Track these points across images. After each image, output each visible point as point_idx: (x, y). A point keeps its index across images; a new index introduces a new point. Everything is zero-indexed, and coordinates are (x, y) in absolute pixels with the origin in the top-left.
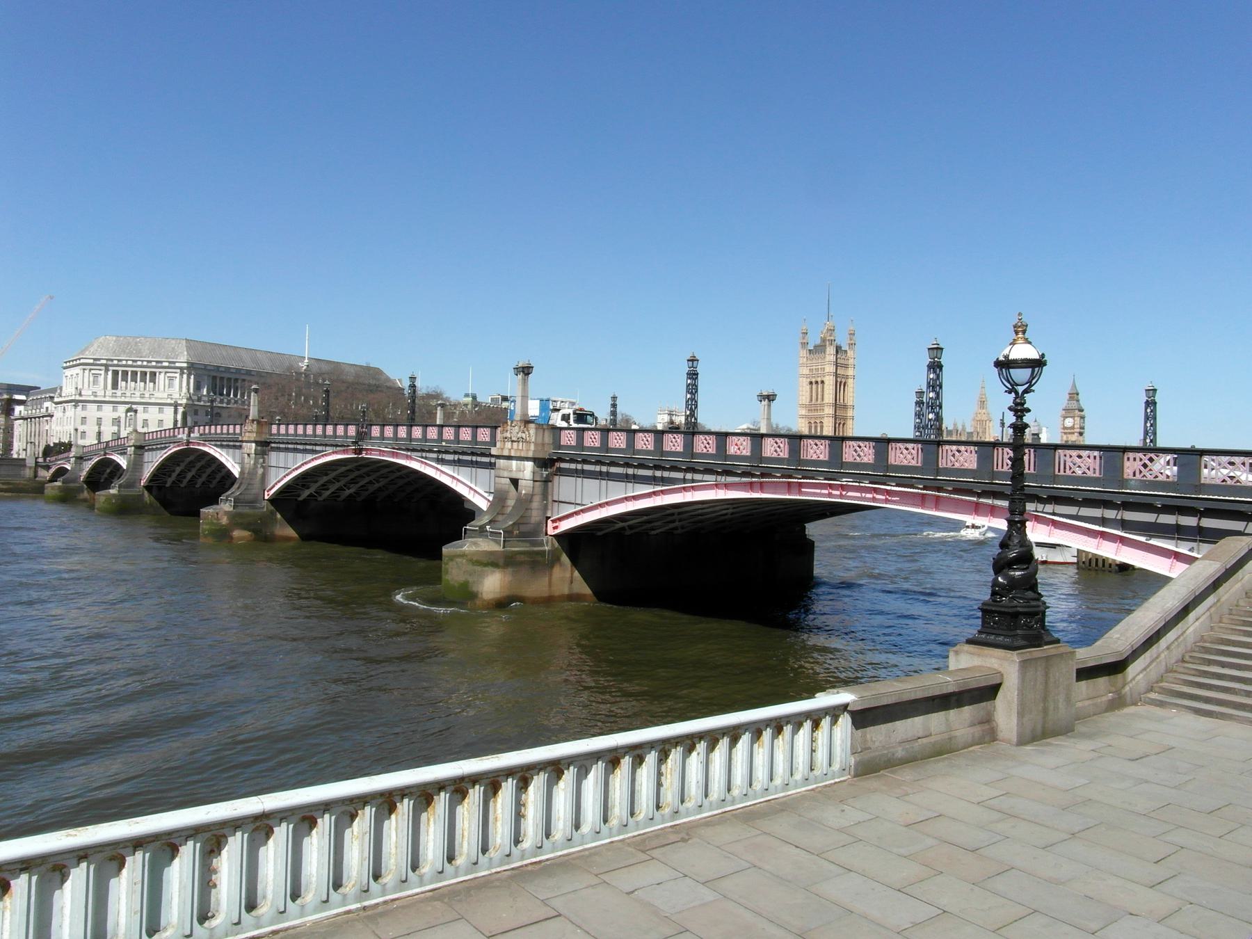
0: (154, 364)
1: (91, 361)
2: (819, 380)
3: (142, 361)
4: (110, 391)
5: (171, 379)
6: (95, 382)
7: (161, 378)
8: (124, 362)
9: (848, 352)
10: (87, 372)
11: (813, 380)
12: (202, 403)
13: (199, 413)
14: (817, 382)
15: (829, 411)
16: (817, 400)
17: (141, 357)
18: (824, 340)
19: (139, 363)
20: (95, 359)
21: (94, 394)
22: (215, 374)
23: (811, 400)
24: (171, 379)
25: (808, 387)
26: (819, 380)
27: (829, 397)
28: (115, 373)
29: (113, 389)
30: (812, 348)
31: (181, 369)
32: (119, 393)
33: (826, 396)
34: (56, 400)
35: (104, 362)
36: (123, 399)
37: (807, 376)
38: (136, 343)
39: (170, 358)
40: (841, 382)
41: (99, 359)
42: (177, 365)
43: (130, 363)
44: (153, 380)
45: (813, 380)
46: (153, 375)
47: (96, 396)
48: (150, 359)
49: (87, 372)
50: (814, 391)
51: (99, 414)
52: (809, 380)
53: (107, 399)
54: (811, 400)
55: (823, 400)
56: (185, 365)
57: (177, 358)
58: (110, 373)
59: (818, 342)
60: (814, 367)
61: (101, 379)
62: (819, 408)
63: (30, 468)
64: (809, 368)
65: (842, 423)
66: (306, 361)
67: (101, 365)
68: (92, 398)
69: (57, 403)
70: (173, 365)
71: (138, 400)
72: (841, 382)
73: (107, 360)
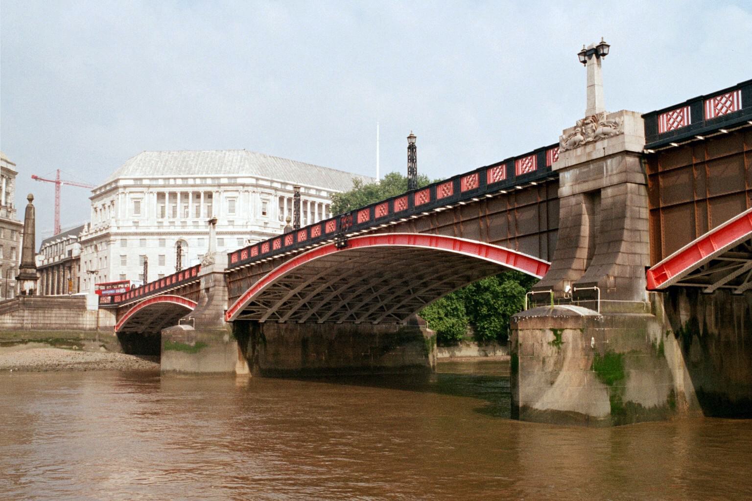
0: (209, 181)
1: (131, 182)
3: (194, 178)
19: (191, 182)
24: (232, 200)
28: (161, 196)
34: (83, 239)
36: (172, 229)
39: (229, 173)
42: (239, 181)
43: (179, 182)
46: (209, 195)
48: (204, 175)
53: (153, 230)
57: (238, 173)
63: (92, 312)
69: (82, 243)
73: (151, 179)
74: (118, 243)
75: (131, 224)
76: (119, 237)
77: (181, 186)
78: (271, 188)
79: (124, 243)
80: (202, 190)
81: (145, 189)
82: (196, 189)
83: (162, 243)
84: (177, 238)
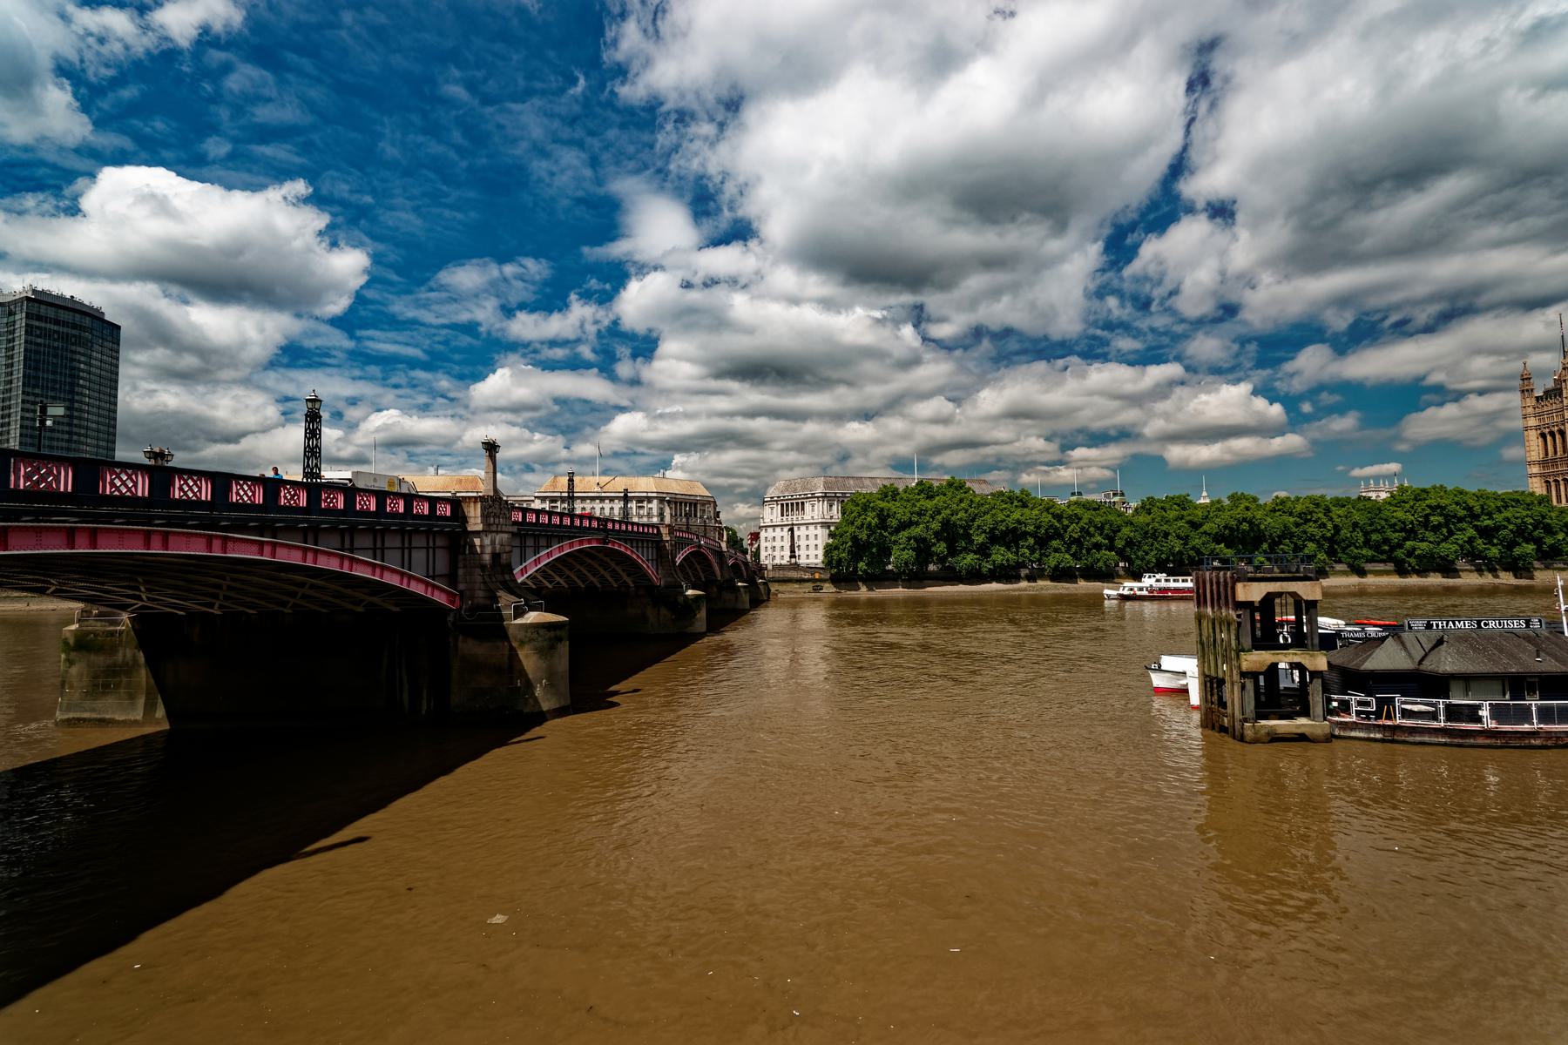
4: (779, 519)
5: (813, 505)
7: (807, 506)
16: (1556, 453)
23: (1547, 454)
24: (813, 505)
28: (782, 505)
30: (1541, 394)
31: (818, 497)
32: (785, 518)
37: (1537, 428)
44: (803, 509)
46: (803, 503)
52: (1539, 432)
54: (1547, 454)
59: (1550, 385)
83: (782, 530)
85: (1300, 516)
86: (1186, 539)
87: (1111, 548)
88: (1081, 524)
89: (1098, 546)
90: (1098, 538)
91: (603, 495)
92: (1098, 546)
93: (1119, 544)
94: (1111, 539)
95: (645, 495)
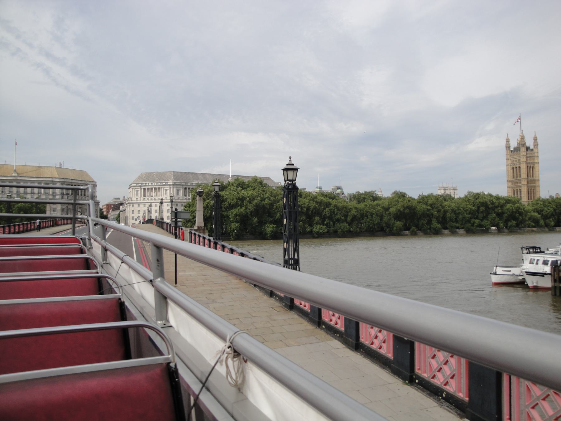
1: (135, 185)
2: (517, 166)
3: (155, 183)
4: (143, 198)
6: (137, 194)
8: (148, 184)
9: (534, 149)
10: (134, 189)
11: (514, 167)
12: (179, 201)
13: (178, 205)
14: (516, 167)
15: (524, 183)
16: (517, 177)
17: (154, 181)
18: (519, 144)
19: (154, 184)
20: (137, 184)
21: (137, 200)
22: (186, 187)
23: (514, 177)
25: (512, 171)
26: (517, 166)
27: (524, 175)
28: (144, 189)
29: (144, 197)
32: (146, 198)
33: (522, 175)
35: (140, 185)
36: (147, 201)
38: (153, 175)
40: (530, 167)
41: (138, 184)
43: (150, 184)
45: (514, 167)
46: (159, 189)
47: (137, 200)
48: (158, 182)
49: (134, 189)
50: (515, 173)
51: (139, 209)
52: (512, 167)
54: (514, 177)
55: (520, 177)
56: (171, 183)
58: (143, 189)
59: (516, 145)
60: (514, 160)
61: (139, 192)
62: (518, 182)
64: (511, 160)
65: (533, 189)
66: (230, 177)
67: (139, 186)
68: (136, 202)
70: (167, 184)
71: (153, 201)
72: (530, 167)
74: (132, 206)
75: (135, 199)
76: (131, 204)
77: (150, 186)
78: (181, 185)
79: (133, 206)
80: (157, 187)
81: (140, 187)
82: (155, 187)
84: (149, 204)
85: (431, 205)
86: (382, 217)
87: (346, 220)
88: (331, 207)
89: (338, 220)
90: (338, 216)
91: (19, 178)
92: (338, 220)
93: (349, 218)
94: (346, 216)
95: (50, 180)
